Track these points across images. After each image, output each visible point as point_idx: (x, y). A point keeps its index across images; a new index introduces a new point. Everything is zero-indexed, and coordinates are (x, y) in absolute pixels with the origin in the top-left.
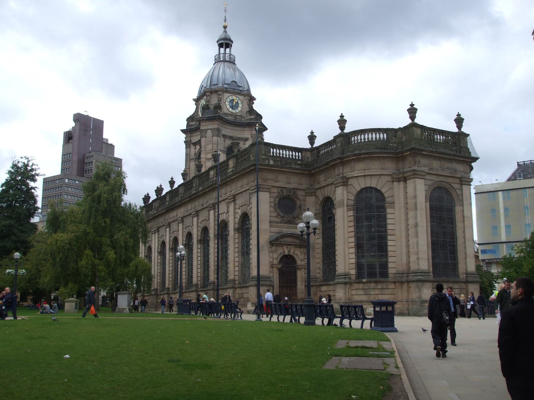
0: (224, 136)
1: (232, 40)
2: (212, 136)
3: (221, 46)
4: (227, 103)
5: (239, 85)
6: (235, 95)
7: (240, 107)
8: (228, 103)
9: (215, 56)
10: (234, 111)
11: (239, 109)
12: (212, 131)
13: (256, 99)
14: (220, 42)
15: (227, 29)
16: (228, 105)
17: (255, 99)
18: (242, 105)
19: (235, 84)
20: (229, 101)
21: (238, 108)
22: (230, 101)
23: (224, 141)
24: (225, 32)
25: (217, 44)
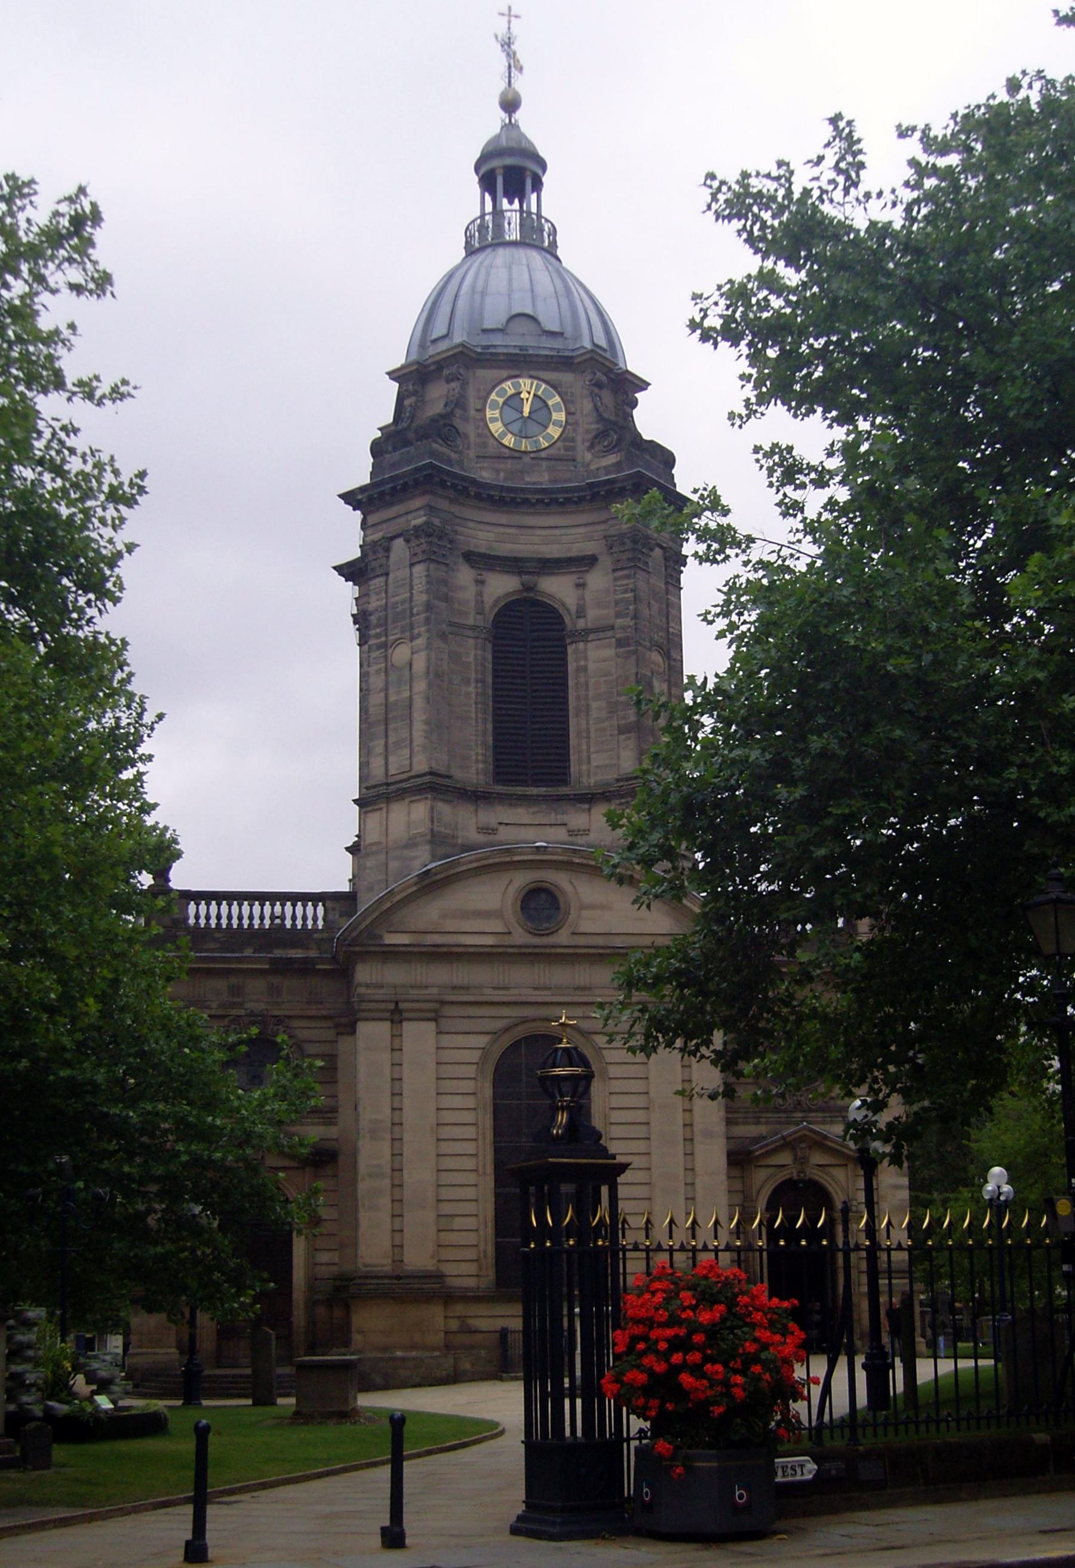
0: (472, 558)
1: (542, 154)
2: (412, 565)
3: (487, 183)
4: (489, 414)
5: (547, 329)
6: (532, 373)
7: (557, 423)
8: (497, 413)
9: (467, 228)
10: (525, 445)
11: (554, 432)
12: (407, 541)
13: (649, 384)
14: (482, 172)
15: (519, 116)
16: (496, 420)
17: (643, 385)
18: (569, 413)
19: (530, 325)
20: (501, 401)
21: (546, 427)
22: (505, 403)
23: (480, 582)
24: (510, 127)
25: (476, 179)
